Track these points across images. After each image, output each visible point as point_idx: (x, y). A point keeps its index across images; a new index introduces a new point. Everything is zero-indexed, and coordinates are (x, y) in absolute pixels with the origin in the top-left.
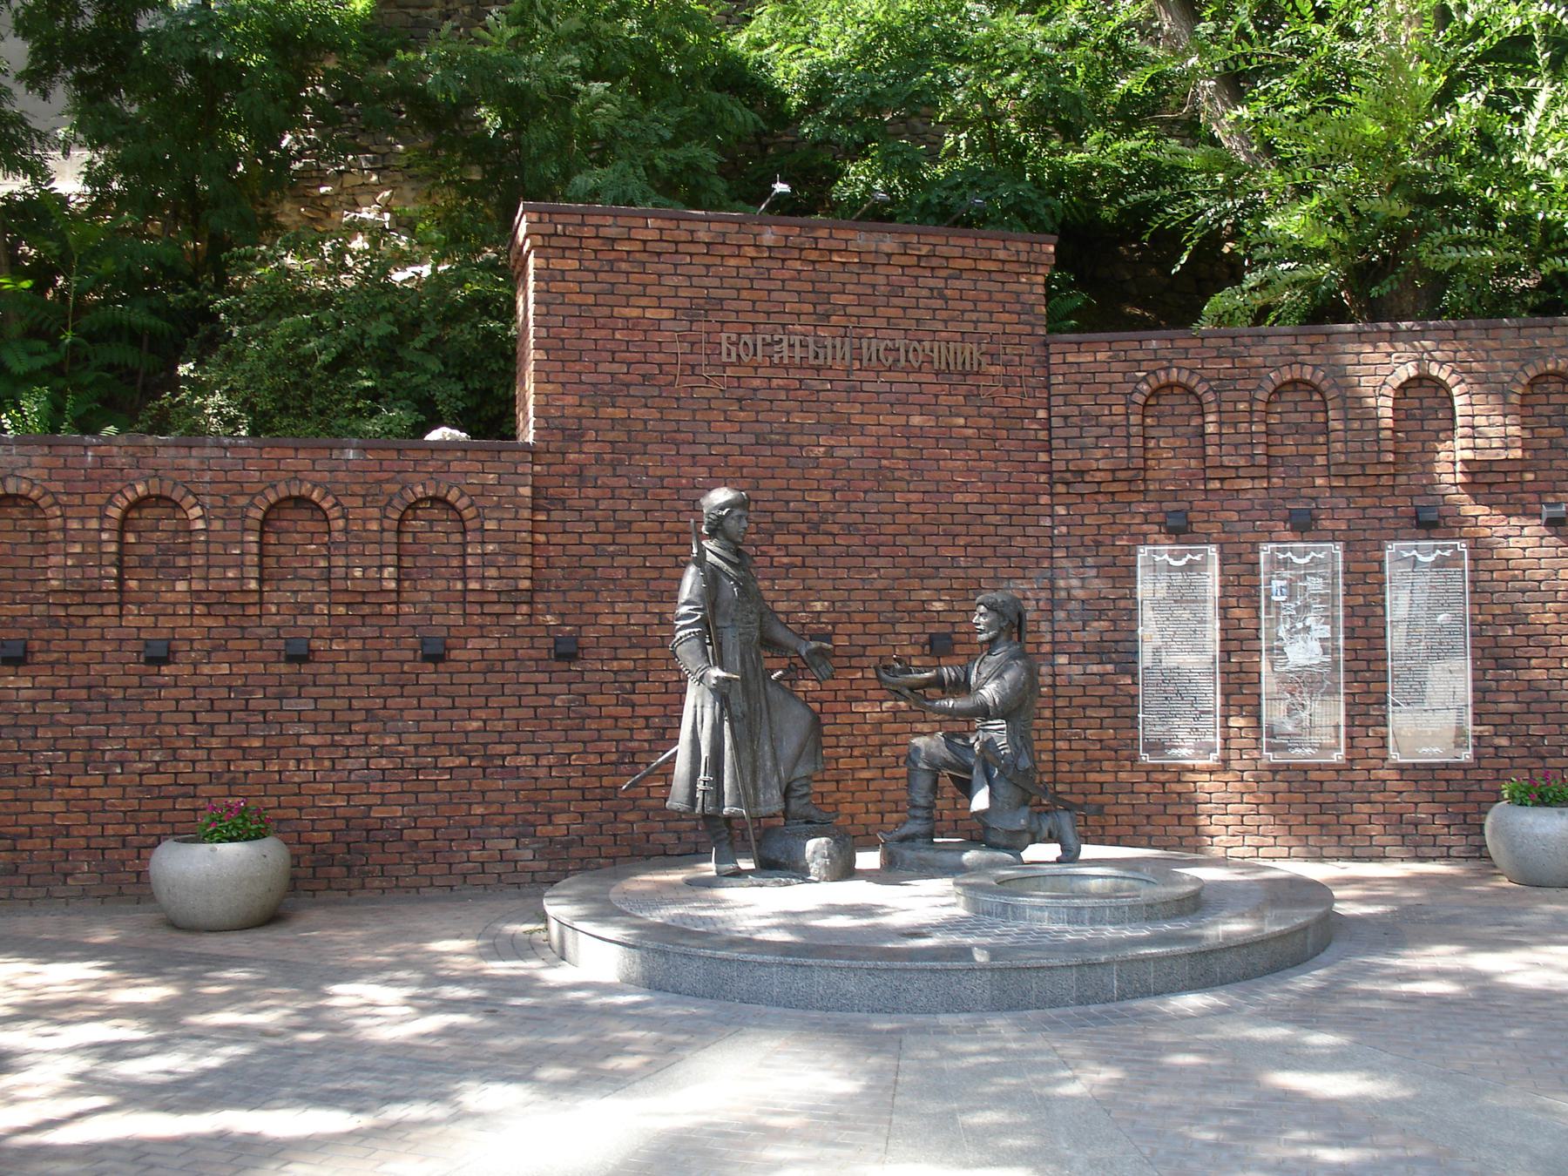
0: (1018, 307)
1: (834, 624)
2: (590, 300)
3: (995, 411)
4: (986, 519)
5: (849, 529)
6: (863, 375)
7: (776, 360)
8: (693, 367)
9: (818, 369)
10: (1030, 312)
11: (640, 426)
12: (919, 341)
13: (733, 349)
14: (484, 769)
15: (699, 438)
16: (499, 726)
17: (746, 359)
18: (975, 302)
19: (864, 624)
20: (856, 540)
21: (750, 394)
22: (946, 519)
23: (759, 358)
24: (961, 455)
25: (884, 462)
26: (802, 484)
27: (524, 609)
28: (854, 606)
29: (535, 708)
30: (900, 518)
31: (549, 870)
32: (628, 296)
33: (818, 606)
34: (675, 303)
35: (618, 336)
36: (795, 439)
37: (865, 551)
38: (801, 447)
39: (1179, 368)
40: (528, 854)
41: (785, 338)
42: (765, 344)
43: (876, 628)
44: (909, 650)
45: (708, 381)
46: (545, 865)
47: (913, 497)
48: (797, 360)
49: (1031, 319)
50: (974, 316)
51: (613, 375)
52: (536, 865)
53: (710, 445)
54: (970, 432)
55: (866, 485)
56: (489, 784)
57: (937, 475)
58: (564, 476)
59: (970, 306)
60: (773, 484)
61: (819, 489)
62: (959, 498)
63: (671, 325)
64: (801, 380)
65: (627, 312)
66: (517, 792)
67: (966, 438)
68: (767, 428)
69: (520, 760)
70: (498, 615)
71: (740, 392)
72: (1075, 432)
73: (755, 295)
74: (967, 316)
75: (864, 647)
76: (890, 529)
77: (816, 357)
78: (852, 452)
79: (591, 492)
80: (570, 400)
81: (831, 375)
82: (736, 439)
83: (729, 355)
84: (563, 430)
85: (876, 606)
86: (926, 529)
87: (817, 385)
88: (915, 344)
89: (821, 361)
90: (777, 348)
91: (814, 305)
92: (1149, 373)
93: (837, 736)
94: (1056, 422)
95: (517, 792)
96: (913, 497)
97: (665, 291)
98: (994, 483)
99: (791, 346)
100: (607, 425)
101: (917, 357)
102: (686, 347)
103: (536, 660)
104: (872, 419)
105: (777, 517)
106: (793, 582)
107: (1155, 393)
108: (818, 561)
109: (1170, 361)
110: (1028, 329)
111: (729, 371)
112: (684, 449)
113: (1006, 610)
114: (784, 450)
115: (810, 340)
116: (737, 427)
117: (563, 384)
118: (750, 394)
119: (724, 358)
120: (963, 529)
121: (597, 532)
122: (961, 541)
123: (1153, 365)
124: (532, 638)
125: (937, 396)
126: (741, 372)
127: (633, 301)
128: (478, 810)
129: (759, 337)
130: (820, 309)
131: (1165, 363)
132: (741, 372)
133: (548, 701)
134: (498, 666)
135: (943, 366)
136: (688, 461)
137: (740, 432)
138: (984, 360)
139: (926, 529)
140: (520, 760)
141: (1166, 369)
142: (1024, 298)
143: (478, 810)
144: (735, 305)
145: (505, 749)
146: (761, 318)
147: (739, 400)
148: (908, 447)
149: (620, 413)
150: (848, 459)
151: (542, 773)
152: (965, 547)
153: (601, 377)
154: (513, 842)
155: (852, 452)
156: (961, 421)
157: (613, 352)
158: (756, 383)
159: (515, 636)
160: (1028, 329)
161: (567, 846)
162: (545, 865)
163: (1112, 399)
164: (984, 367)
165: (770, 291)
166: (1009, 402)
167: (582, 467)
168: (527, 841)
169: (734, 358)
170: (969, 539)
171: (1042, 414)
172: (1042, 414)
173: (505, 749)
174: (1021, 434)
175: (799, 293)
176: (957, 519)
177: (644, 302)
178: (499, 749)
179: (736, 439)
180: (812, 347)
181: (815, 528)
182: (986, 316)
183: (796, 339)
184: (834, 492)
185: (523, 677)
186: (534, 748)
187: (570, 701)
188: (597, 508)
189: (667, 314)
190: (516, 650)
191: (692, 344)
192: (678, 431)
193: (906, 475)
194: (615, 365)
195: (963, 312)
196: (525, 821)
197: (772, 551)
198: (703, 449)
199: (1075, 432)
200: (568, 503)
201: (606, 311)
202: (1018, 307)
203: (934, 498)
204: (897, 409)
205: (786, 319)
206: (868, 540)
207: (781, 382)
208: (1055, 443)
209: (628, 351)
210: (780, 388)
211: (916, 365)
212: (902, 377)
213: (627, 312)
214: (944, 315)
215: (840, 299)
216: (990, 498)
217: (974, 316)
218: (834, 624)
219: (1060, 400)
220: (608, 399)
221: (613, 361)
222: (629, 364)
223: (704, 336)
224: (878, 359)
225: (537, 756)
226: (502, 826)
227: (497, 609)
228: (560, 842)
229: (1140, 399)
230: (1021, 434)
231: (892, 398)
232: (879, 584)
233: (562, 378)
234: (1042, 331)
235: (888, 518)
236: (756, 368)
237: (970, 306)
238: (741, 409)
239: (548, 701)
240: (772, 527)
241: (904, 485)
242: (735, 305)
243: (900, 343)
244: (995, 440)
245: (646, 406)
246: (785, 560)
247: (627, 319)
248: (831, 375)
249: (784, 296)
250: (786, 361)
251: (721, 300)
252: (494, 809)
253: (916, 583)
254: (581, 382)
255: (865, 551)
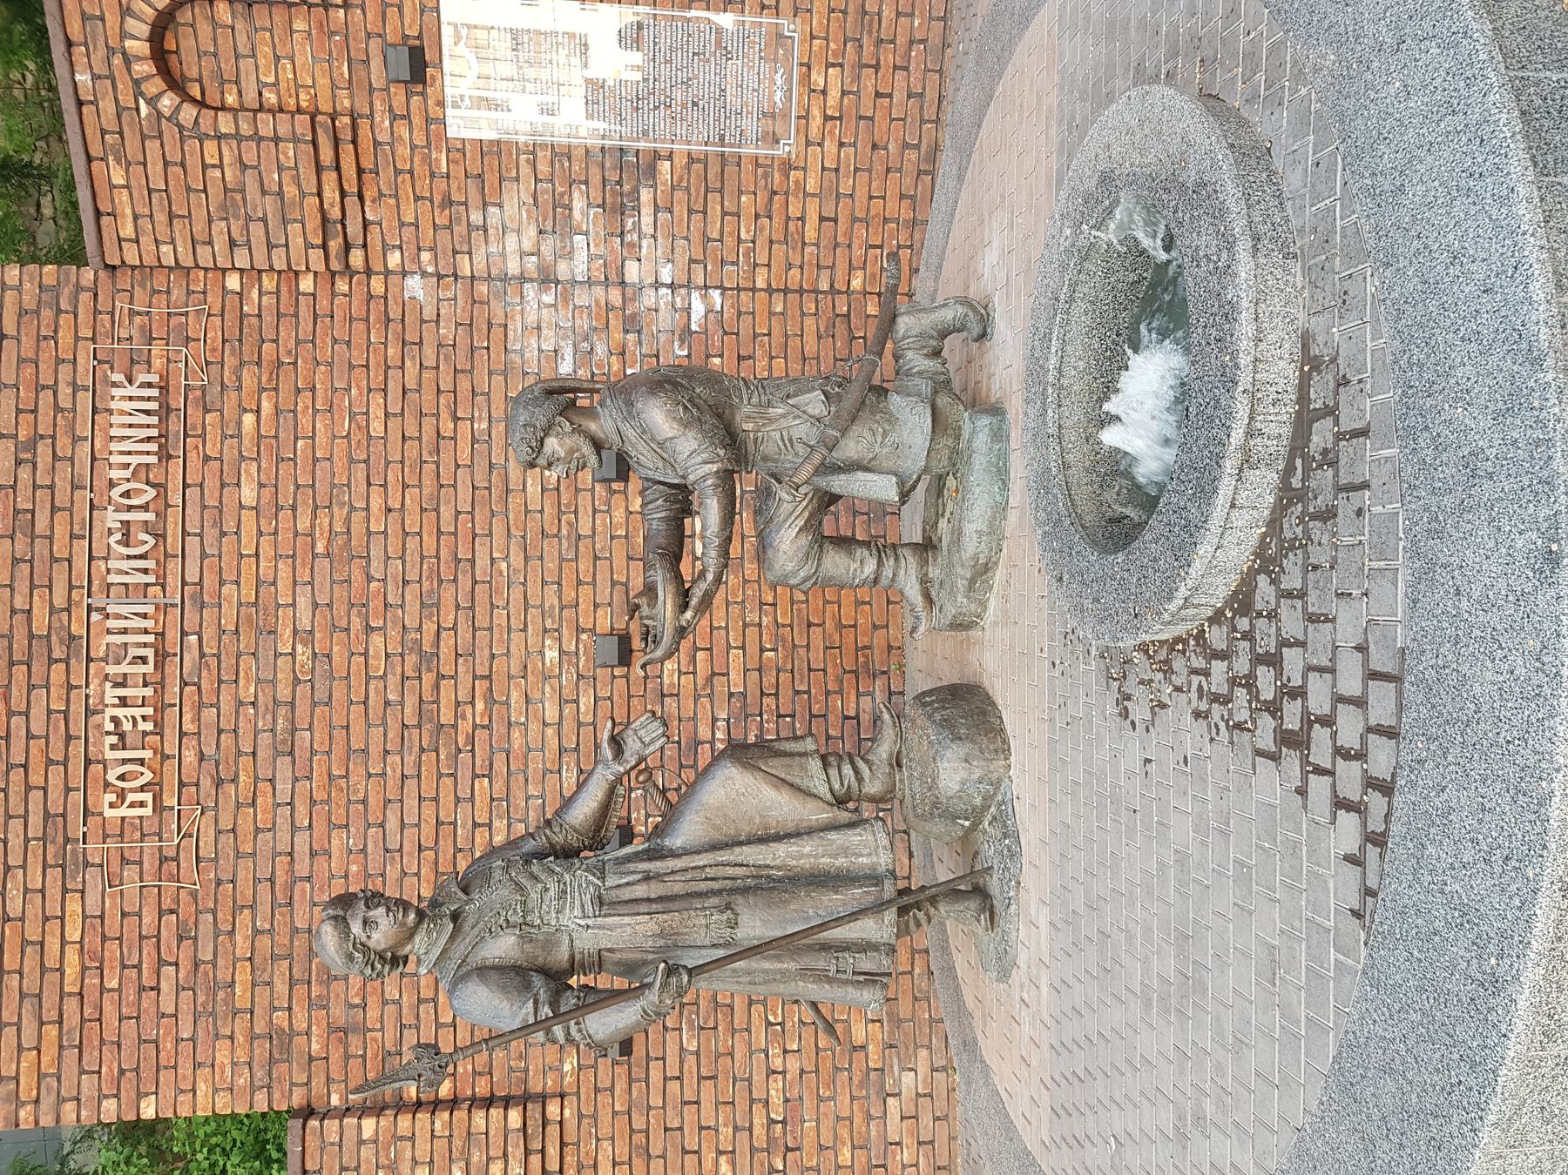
0: (47, 314)
1: (579, 630)
2: (51, 1031)
3: (230, 361)
4: (411, 384)
5: (429, 606)
6: (173, 581)
7: (149, 726)
8: (163, 860)
9: (162, 657)
10: (56, 290)
11: (264, 942)
12: (112, 484)
13: (131, 797)
14: (788, 1149)
15: (284, 846)
16: (726, 1132)
17: (148, 776)
18: (40, 387)
19: (579, 583)
20: (448, 594)
21: (209, 766)
22: (412, 449)
23: (147, 754)
24: (305, 421)
25: (320, 548)
26: (357, 681)
27: (553, 1109)
28: (552, 599)
29: (700, 1078)
30: (412, 524)
31: (929, 1048)
32: (43, 970)
33: (552, 655)
34: (54, 892)
35: (114, 984)
36: (284, 693)
37: (465, 582)
38: (297, 681)
39: (124, 35)
40: (908, 1077)
41: (110, 712)
42: (122, 744)
43: (584, 565)
44: (619, 515)
45: (188, 835)
46: (923, 1053)
47: (376, 502)
48: (149, 692)
49: (66, 292)
50: (65, 391)
51: (179, 989)
52: (923, 1068)
53: (294, 829)
54: (267, 406)
55: (358, 577)
56: (809, 1143)
57: (340, 462)
58: (347, 1057)
59: (46, 397)
60: (357, 728)
61: (366, 654)
62: (377, 428)
63: (92, 899)
64: (184, 684)
65: (72, 970)
66: (820, 1099)
67: (277, 411)
68: (265, 739)
69: (776, 1098)
70: (563, 1144)
71: (206, 783)
72: (257, 230)
73: (36, 761)
74: (65, 403)
75: (613, 583)
76: (429, 541)
77: (144, 660)
78: (303, 602)
79: (373, 1014)
80: (223, 1056)
81: (173, 635)
82: (284, 788)
83: (142, 804)
84: (272, 1061)
85: (551, 565)
86: (428, 481)
87: (191, 657)
88: (115, 493)
89: (149, 653)
90: (127, 726)
91: (52, 661)
92: (138, 94)
93: (745, 626)
94: (242, 261)
95: (820, 1099)
96: (376, 502)
97: (34, 910)
98: (351, 367)
99: (123, 702)
100: (262, 994)
101: (139, 492)
102: (130, 872)
103: (630, 1082)
104: (248, 566)
105: (411, 720)
106: (514, 695)
107: (175, 84)
108: (482, 655)
109: (111, 51)
110: (85, 297)
111: (170, 800)
112: (302, 868)
113: (541, 421)
114: (302, 709)
115: (111, 669)
116: (264, 787)
117: (197, 1066)
118: (209, 766)
119: (147, 811)
120: (428, 423)
121: (435, 1001)
122: (447, 427)
123: (124, 86)
124: (597, 1090)
125: (207, 459)
126: (171, 782)
127: (52, 962)
128: (845, 1156)
129: (110, 755)
130: (58, 653)
131: (117, 61)
132: (171, 782)
133: (691, 1061)
134: (639, 1139)
135: (154, 447)
136: (321, 861)
137: (272, 781)
138: (143, 378)
139: (428, 481)
140: (776, 1098)
141: (127, 60)
142: (29, 301)
143: (845, 1156)
144: (55, 794)
145: (759, 1121)
146: (77, 749)
147: (219, 782)
148: (294, 508)
149: (243, 975)
150: (315, 605)
151: (793, 1064)
152: (456, 419)
153: (183, 1007)
154: (890, 1101)
155: (303, 602)
156: (248, 419)
157: (142, 989)
158: (190, 757)
159: (595, 1117)
160: (85, 297)
161: (897, 1022)
162: (923, 1053)
163: (193, 162)
164: (155, 379)
165: (30, 736)
166: (215, 335)
167: (332, 1029)
168: (889, 1082)
169: (148, 797)
170: (445, 414)
171: (233, 282)
172: (233, 282)
173: (759, 1121)
174: (269, 319)
175: (31, 688)
176: (411, 431)
177: (53, 944)
178: (759, 1130)
179: (284, 788)
180: (124, 668)
181: (428, 659)
182: (65, 371)
183: (111, 694)
184: (369, 629)
185: (656, 1101)
186: (758, 1078)
187: (691, 1028)
188: (398, 1003)
189: (73, 905)
190: (615, 1113)
191: (124, 861)
192: (272, 881)
193: (340, 513)
194: (164, 985)
195: (58, 409)
196: (861, 1085)
197: (465, 727)
198: (302, 840)
199: (257, 230)
200: (389, 1046)
201: (71, 1005)
202: (47, 314)
203: (377, 465)
204: (229, 526)
205: (78, 709)
206: (446, 574)
207: (187, 717)
208: (280, 264)
209: (138, 967)
210: (198, 719)
211: (152, 493)
212: (174, 517)
213: (72, 970)
214: (63, 441)
215: (40, 622)
216: (377, 378)
217: (65, 391)
218: (579, 630)
219: (204, 253)
220: (221, 995)
221: (157, 989)
222: (161, 962)
223: (111, 844)
224: (143, 557)
225: (771, 1072)
226: (869, 1117)
227: (553, 1151)
228: (891, 1033)
229: (188, 113)
230: (269, 319)
231: (211, 534)
232: (517, 559)
233: (185, 1069)
234: (88, 275)
235: (412, 543)
236: (165, 757)
237: (46, 397)
238: (235, 780)
239: (691, 1061)
240: (427, 727)
241: (358, 517)
242: (55, 794)
243: (112, 518)
244: (280, 364)
245: (232, 932)
246: (480, 706)
247: (84, 969)
248: (173, 635)
249: (38, 713)
250: (150, 711)
251: (47, 815)
252: (844, 1133)
253: (515, 501)
254: (192, 1039)
255: (465, 582)
